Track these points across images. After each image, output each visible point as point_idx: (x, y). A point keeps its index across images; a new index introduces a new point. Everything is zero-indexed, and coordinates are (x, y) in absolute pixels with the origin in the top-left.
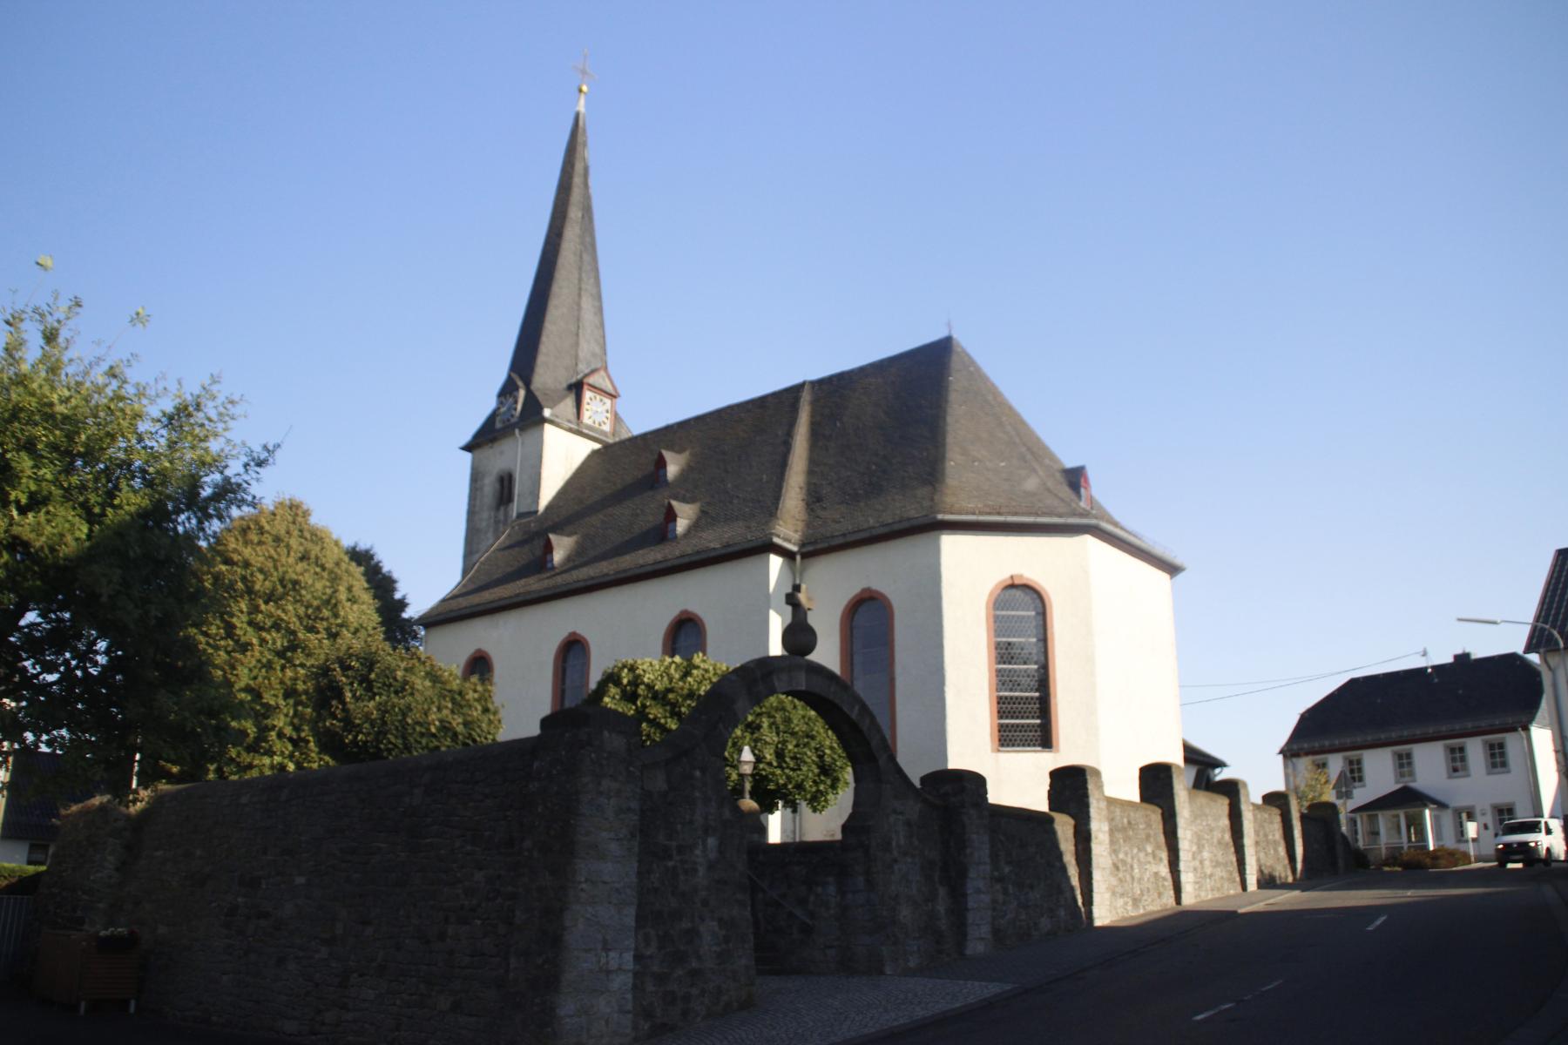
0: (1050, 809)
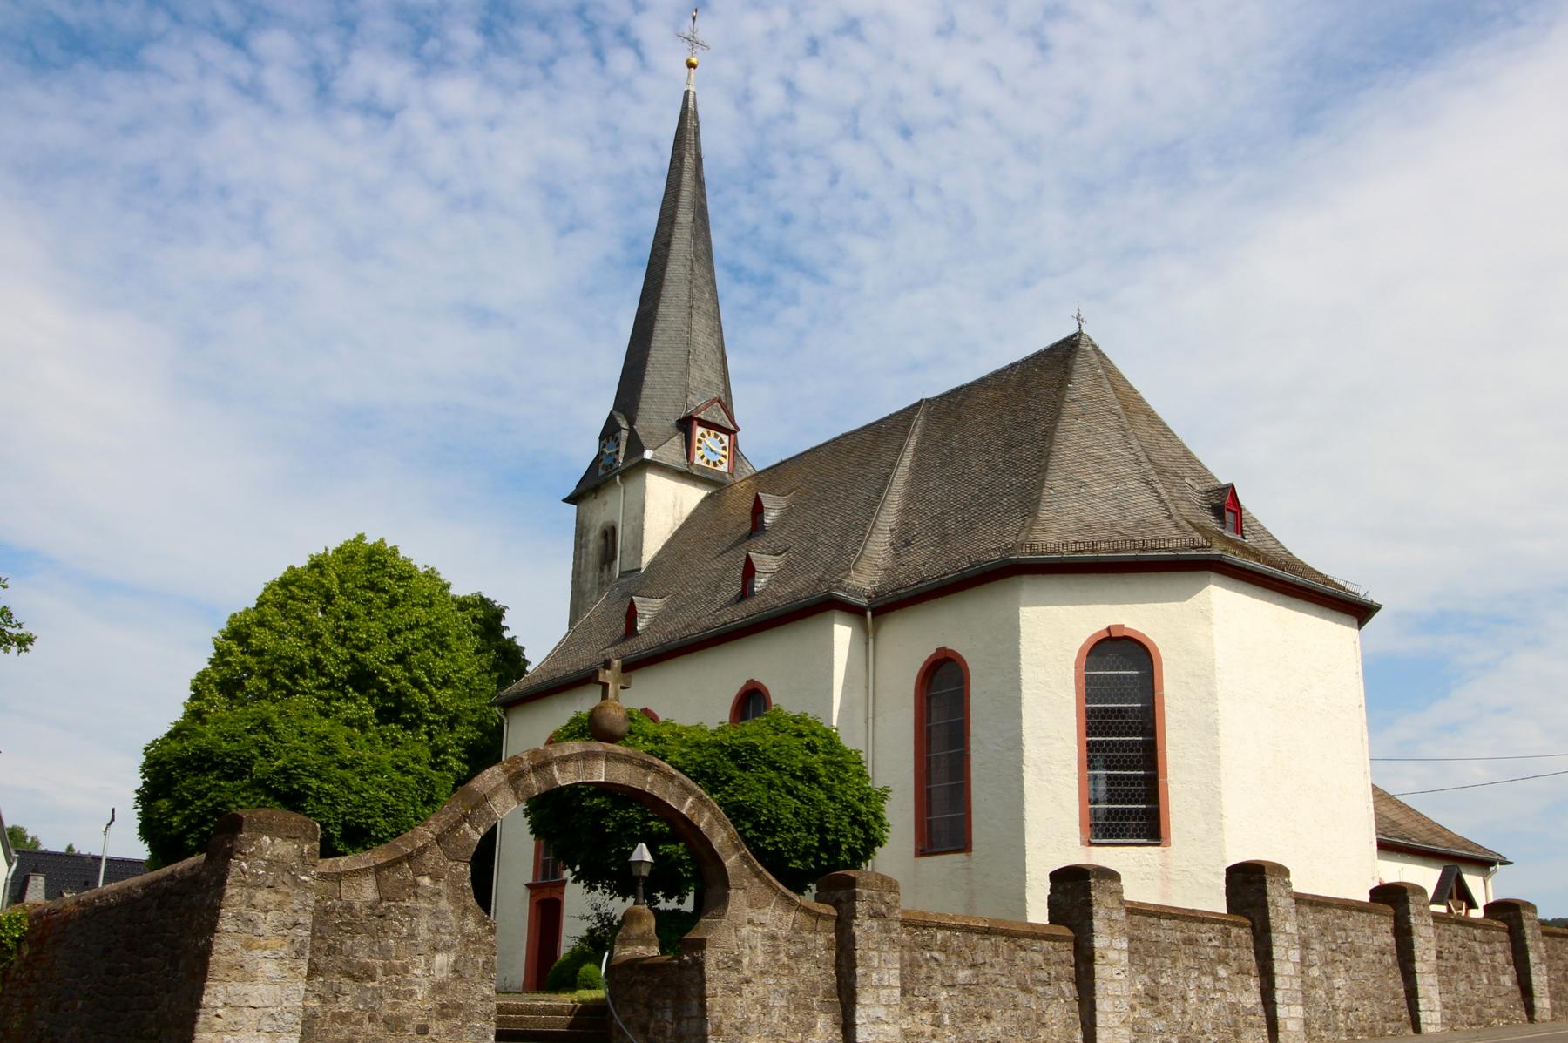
0: (1052, 920)
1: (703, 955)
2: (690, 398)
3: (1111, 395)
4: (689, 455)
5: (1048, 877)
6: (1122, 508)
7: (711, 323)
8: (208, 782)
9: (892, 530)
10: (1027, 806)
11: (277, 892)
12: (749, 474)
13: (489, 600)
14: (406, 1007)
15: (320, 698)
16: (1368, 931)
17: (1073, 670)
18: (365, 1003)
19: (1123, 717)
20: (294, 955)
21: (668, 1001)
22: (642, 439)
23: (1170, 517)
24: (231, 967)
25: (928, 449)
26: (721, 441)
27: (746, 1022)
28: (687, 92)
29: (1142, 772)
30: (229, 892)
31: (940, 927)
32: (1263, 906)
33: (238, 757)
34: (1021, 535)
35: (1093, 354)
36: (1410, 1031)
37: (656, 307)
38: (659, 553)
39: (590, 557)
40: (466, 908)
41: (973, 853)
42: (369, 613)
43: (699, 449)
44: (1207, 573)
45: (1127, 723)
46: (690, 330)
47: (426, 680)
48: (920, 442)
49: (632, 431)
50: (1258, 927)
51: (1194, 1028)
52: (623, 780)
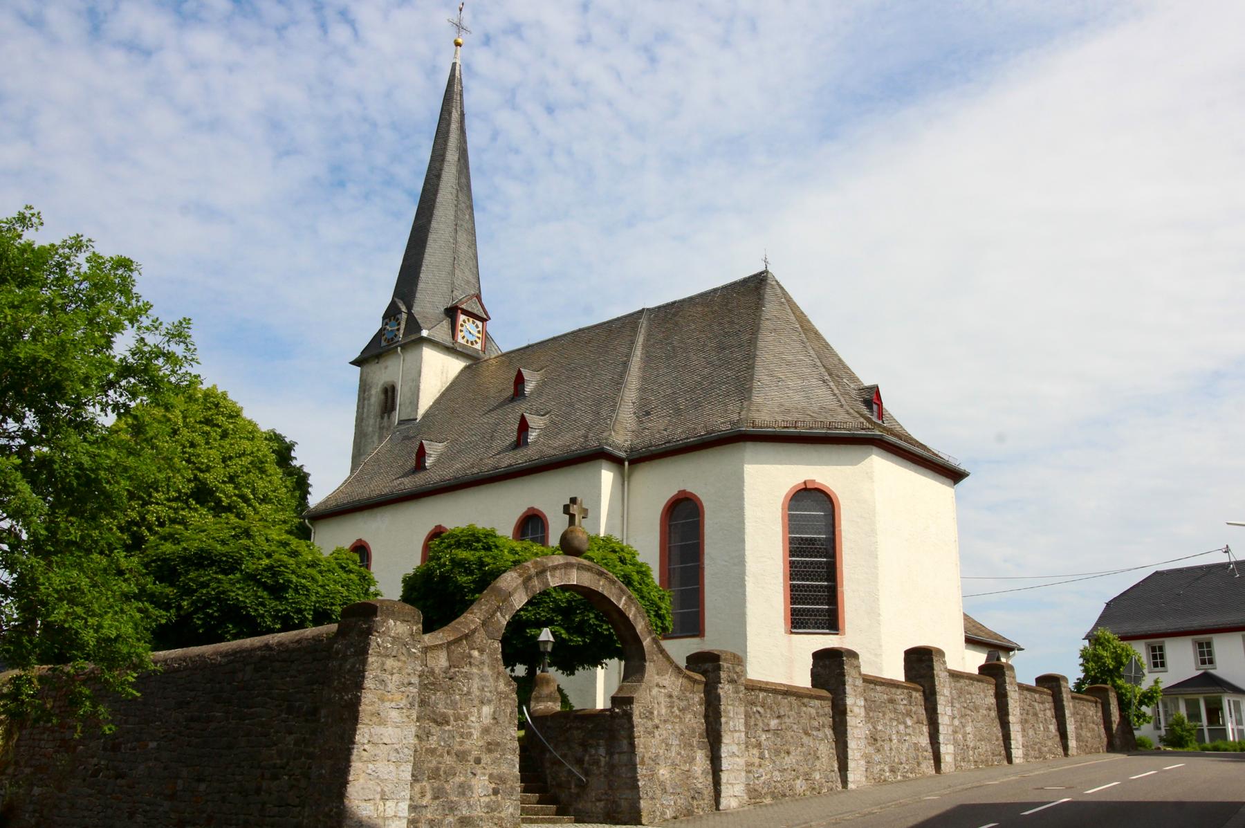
0: (813, 685)
1: (631, 708)
2: (455, 292)
3: (792, 317)
4: (454, 336)
5: (902, 656)
6: (808, 398)
7: (470, 238)
8: (209, 575)
9: (634, 403)
10: (748, 605)
11: (399, 661)
12: (496, 354)
13: (280, 435)
14: (468, 744)
15: (170, 508)
16: (982, 695)
17: (780, 510)
18: (445, 742)
19: (813, 544)
20: (409, 706)
21: (601, 741)
22: (419, 321)
23: (842, 406)
24: (373, 715)
25: (653, 345)
26: (477, 327)
27: (657, 756)
28: (454, 64)
29: (826, 583)
30: (370, 659)
31: (761, 689)
32: (931, 677)
33: (232, 557)
34: (742, 413)
35: (777, 287)
36: (1005, 763)
37: (430, 222)
38: (431, 407)
39: (372, 408)
40: (499, 673)
41: (705, 638)
42: (207, 443)
43: (461, 331)
44: (871, 446)
45: (816, 548)
46: (456, 242)
47: (252, 496)
48: (647, 340)
49: (410, 315)
50: (927, 692)
51: (896, 760)
52: (586, 584)
